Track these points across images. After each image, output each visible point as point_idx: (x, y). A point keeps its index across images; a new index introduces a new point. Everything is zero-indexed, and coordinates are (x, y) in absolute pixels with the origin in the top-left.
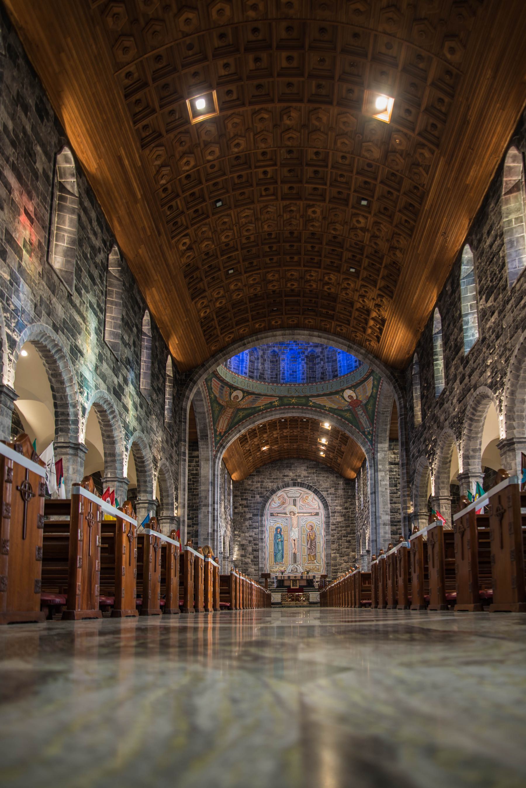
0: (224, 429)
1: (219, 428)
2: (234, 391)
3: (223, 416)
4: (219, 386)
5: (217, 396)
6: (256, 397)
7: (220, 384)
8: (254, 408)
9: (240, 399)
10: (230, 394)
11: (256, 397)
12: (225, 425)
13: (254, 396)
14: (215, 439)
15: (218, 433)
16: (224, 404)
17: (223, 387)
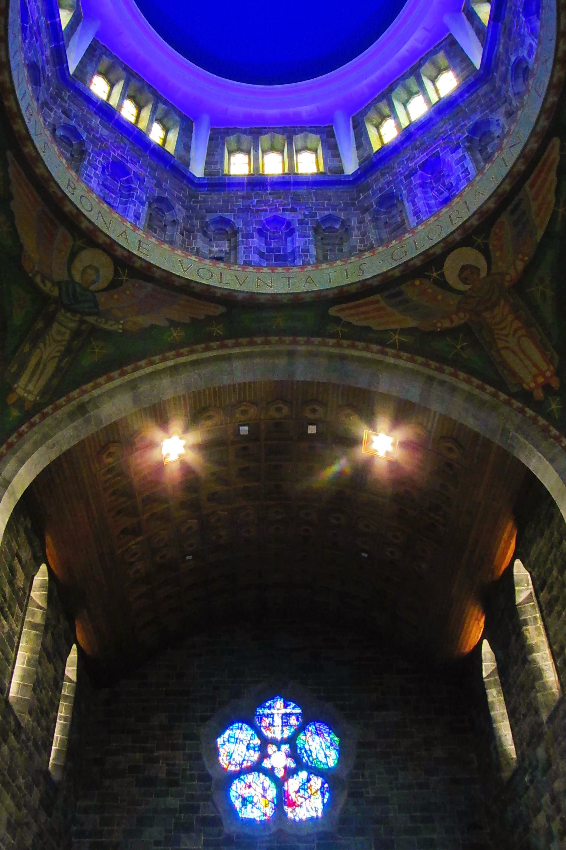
0: (544, 366)
1: (528, 379)
2: (440, 266)
3: (500, 344)
4: (383, 304)
5: (411, 323)
6: (512, 212)
7: (378, 297)
8: (547, 234)
9: (482, 263)
10: (442, 284)
11: (512, 212)
12: (537, 356)
13: (504, 218)
14: (549, 416)
15: (539, 394)
16: (459, 320)
17: (400, 293)
